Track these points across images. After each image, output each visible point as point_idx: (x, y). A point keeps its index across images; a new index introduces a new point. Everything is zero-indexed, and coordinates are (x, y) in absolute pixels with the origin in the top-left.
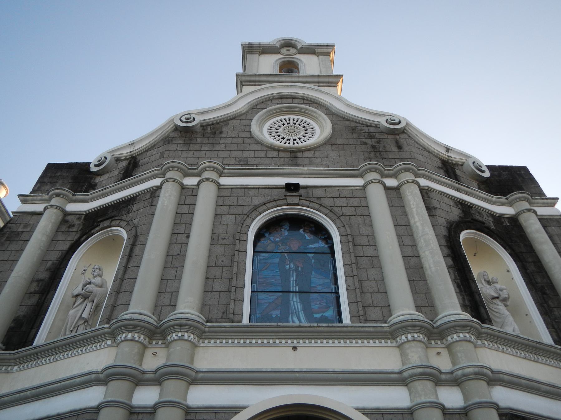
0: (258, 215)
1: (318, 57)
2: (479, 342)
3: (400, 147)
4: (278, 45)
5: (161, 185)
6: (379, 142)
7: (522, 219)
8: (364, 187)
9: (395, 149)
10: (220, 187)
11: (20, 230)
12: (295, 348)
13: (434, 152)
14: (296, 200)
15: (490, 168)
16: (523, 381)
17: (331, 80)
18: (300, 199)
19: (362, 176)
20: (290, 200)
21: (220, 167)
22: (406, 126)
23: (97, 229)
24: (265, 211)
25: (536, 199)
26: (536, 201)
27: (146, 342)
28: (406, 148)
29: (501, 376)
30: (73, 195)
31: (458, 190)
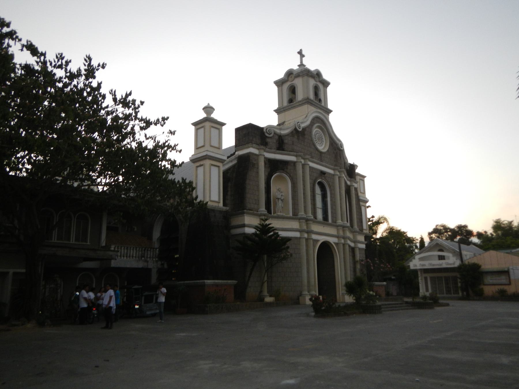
1: (324, 87)
3: (340, 157)
5: (297, 162)
6: (337, 153)
7: (351, 187)
8: (334, 175)
9: (339, 158)
11: (254, 162)
12: (324, 227)
14: (323, 178)
19: (334, 170)
23: (278, 171)
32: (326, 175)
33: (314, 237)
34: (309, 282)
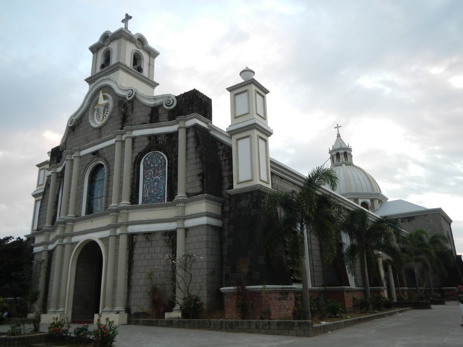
0: (87, 170)
2: (129, 211)
4: (101, 43)
10: (80, 157)
13: (147, 105)
15: (177, 97)
16: (138, 222)
17: (117, 66)
18: (97, 158)
20: (96, 159)
21: (78, 149)
22: (135, 95)
24: (89, 167)
25: (187, 117)
26: (187, 118)
27: (64, 225)
28: (135, 110)
29: (129, 223)
30: (57, 165)
31: (152, 128)
32: (100, 153)
33: (74, 239)
34: (58, 296)
